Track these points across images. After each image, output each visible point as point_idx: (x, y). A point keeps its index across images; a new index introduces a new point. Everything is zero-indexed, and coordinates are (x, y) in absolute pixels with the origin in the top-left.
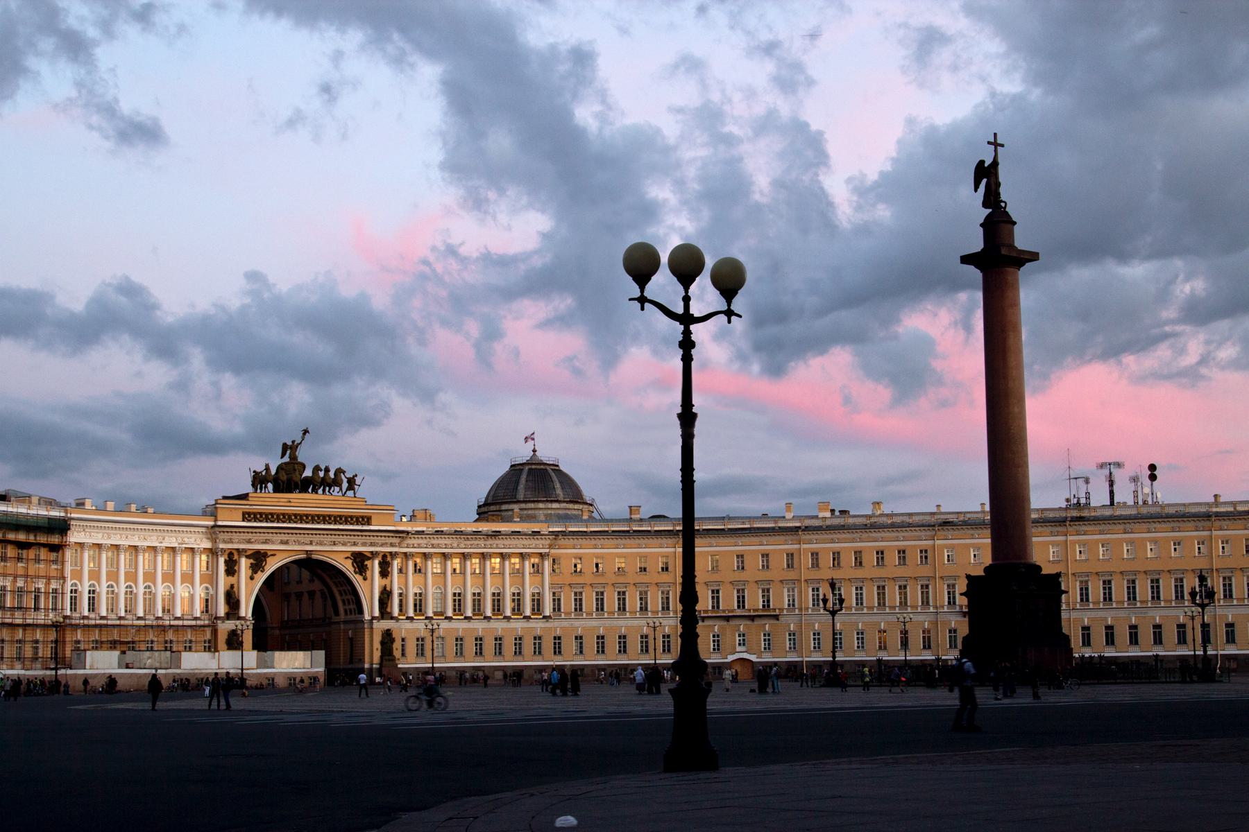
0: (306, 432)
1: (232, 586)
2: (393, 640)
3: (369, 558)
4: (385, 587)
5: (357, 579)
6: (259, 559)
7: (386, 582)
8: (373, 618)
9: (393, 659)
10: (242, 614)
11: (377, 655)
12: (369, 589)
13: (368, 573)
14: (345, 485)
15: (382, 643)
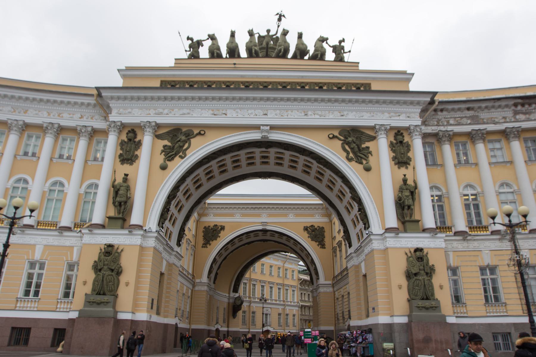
0: (280, 17)
1: (126, 178)
2: (430, 272)
3: (373, 138)
4: (405, 181)
5: (351, 170)
6: (176, 139)
7: (403, 170)
8: (388, 230)
9: (437, 307)
10: (135, 218)
11: (401, 297)
12: (377, 186)
13: (372, 160)
14: (330, 56)
15: (409, 275)
